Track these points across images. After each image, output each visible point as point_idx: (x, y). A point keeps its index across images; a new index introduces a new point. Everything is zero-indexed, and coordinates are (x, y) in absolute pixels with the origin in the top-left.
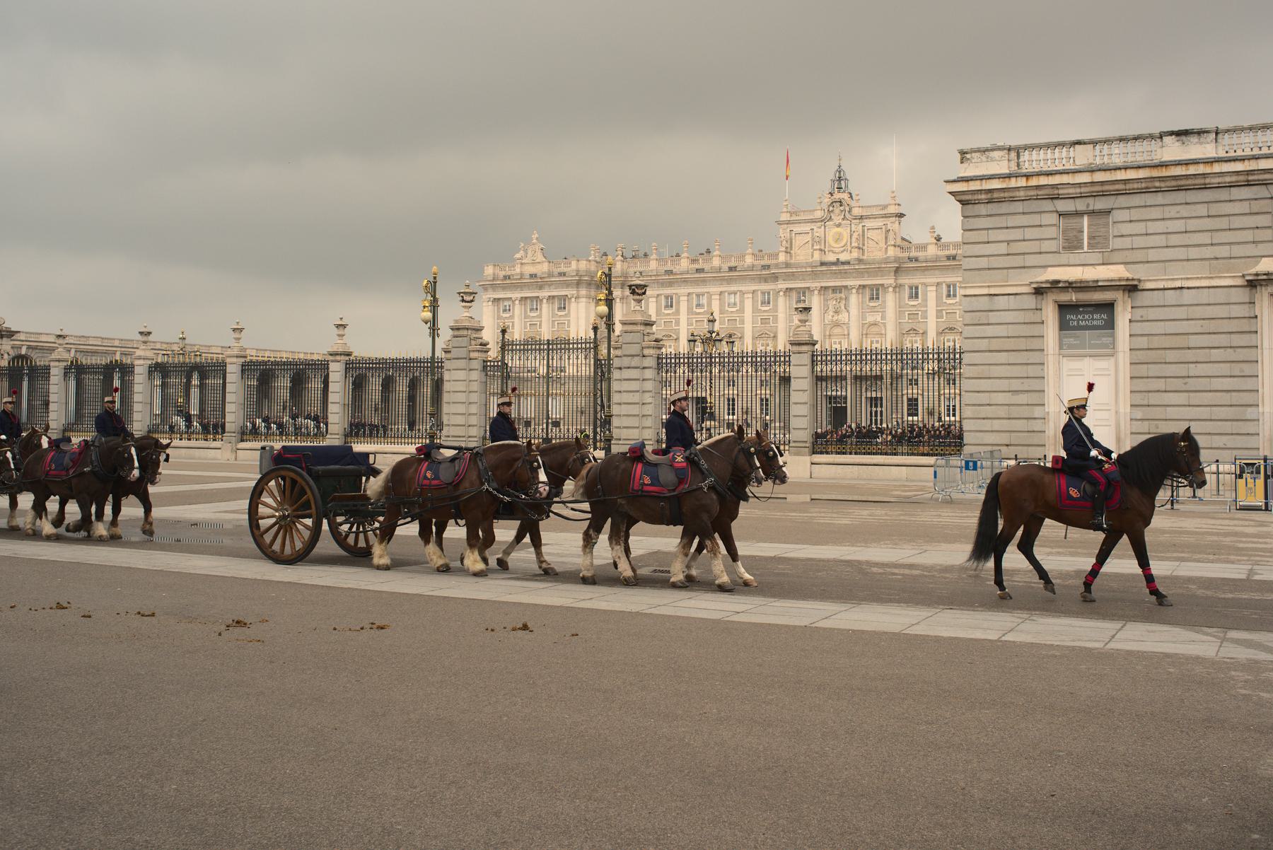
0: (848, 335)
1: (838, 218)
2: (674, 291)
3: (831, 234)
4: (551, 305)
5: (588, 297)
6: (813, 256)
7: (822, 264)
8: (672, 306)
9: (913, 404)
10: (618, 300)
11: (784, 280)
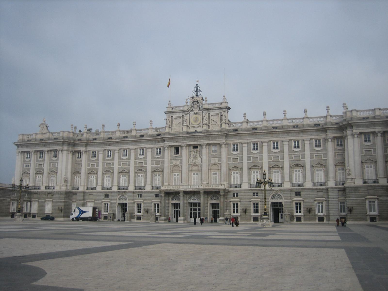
0: (201, 170)
1: (196, 110)
2: (112, 148)
3: (192, 118)
4: (49, 155)
5: (68, 150)
6: (183, 129)
7: (188, 133)
8: (110, 156)
9: (236, 206)
10: (84, 153)
11: (168, 141)
